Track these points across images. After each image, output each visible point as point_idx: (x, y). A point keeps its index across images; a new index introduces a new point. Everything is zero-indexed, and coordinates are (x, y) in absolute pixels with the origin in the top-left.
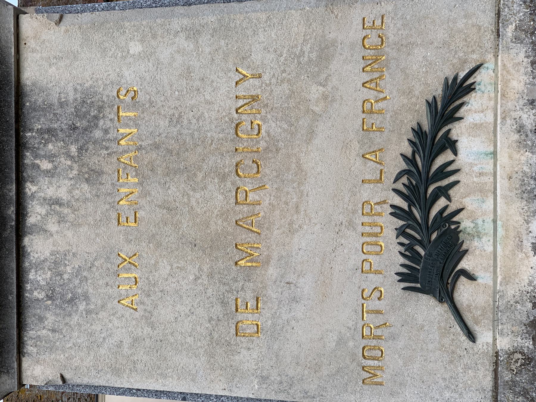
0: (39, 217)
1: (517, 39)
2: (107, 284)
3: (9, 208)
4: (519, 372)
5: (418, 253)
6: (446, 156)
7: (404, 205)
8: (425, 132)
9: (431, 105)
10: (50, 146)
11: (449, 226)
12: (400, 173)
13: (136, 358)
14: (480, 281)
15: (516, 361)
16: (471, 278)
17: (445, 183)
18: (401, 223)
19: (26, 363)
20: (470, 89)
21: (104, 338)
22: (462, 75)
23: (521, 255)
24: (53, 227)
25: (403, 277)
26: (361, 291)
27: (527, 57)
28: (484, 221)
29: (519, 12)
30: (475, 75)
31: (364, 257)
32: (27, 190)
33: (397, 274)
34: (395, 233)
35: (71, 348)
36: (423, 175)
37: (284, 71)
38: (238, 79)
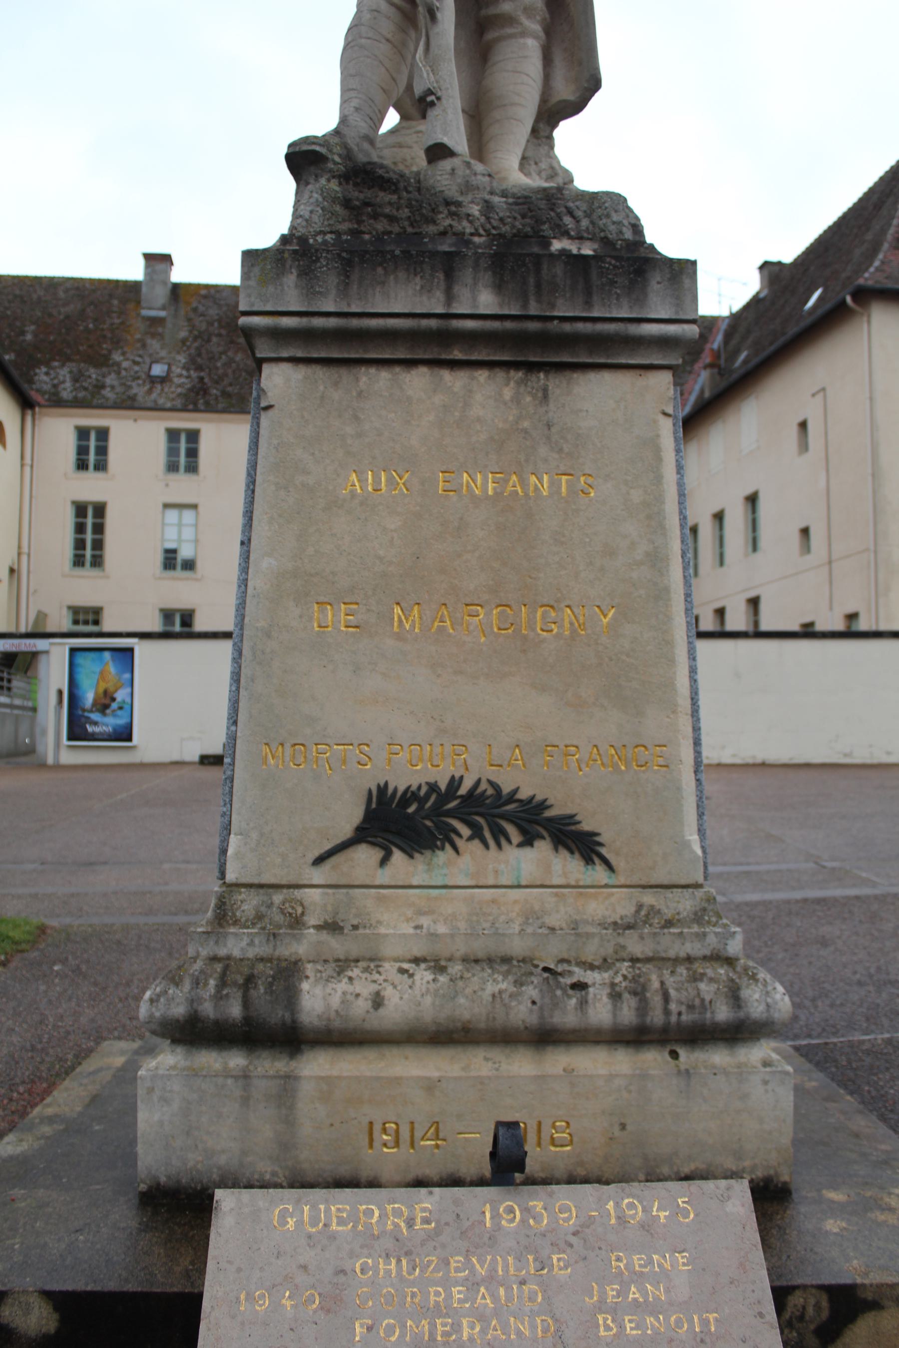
0: (449, 384)
1: (640, 907)
2: (374, 458)
3: (461, 352)
4: (282, 911)
5: (409, 806)
6: (516, 837)
7: (463, 791)
8: (543, 813)
10: (528, 399)
11: (440, 839)
12: (498, 786)
13: (290, 489)
14: (380, 871)
15: (293, 908)
16: (384, 861)
17: (487, 834)
18: (443, 786)
19: (285, 367)
20: (589, 861)
21: (313, 454)
22: (603, 851)
23: (409, 913)
24: (438, 399)
25: (382, 790)
26: (367, 742)
27: (622, 918)
28: (445, 875)
29: (668, 907)
30: (603, 865)
31: (405, 746)
32: (480, 372)
33: (386, 784)
34: (432, 781)
35: (303, 417)
36: (497, 811)
37: (611, 660)
38: (602, 608)
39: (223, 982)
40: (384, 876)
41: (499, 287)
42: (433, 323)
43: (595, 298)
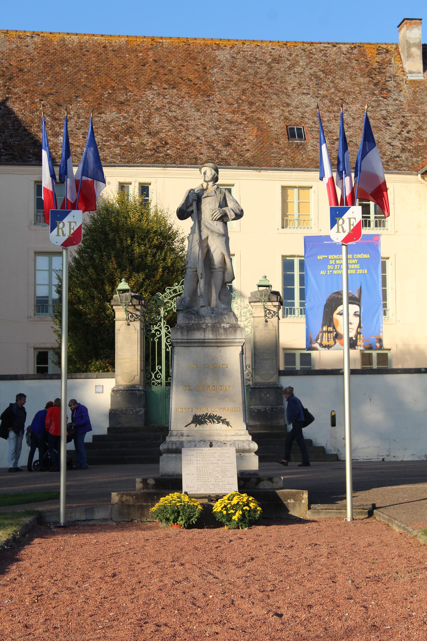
9: (225, 419)
16: (196, 426)
20: (228, 426)
25: (195, 415)
39: (172, 444)
40: (196, 428)
41: (213, 334)
42: (202, 340)
43: (228, 336)
